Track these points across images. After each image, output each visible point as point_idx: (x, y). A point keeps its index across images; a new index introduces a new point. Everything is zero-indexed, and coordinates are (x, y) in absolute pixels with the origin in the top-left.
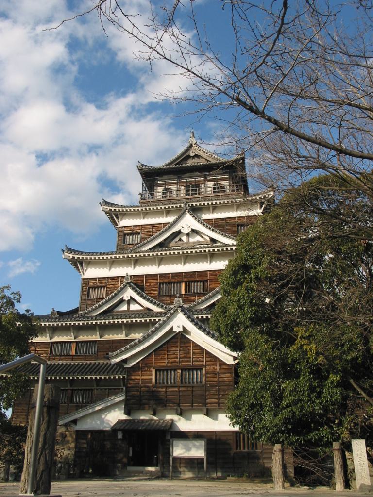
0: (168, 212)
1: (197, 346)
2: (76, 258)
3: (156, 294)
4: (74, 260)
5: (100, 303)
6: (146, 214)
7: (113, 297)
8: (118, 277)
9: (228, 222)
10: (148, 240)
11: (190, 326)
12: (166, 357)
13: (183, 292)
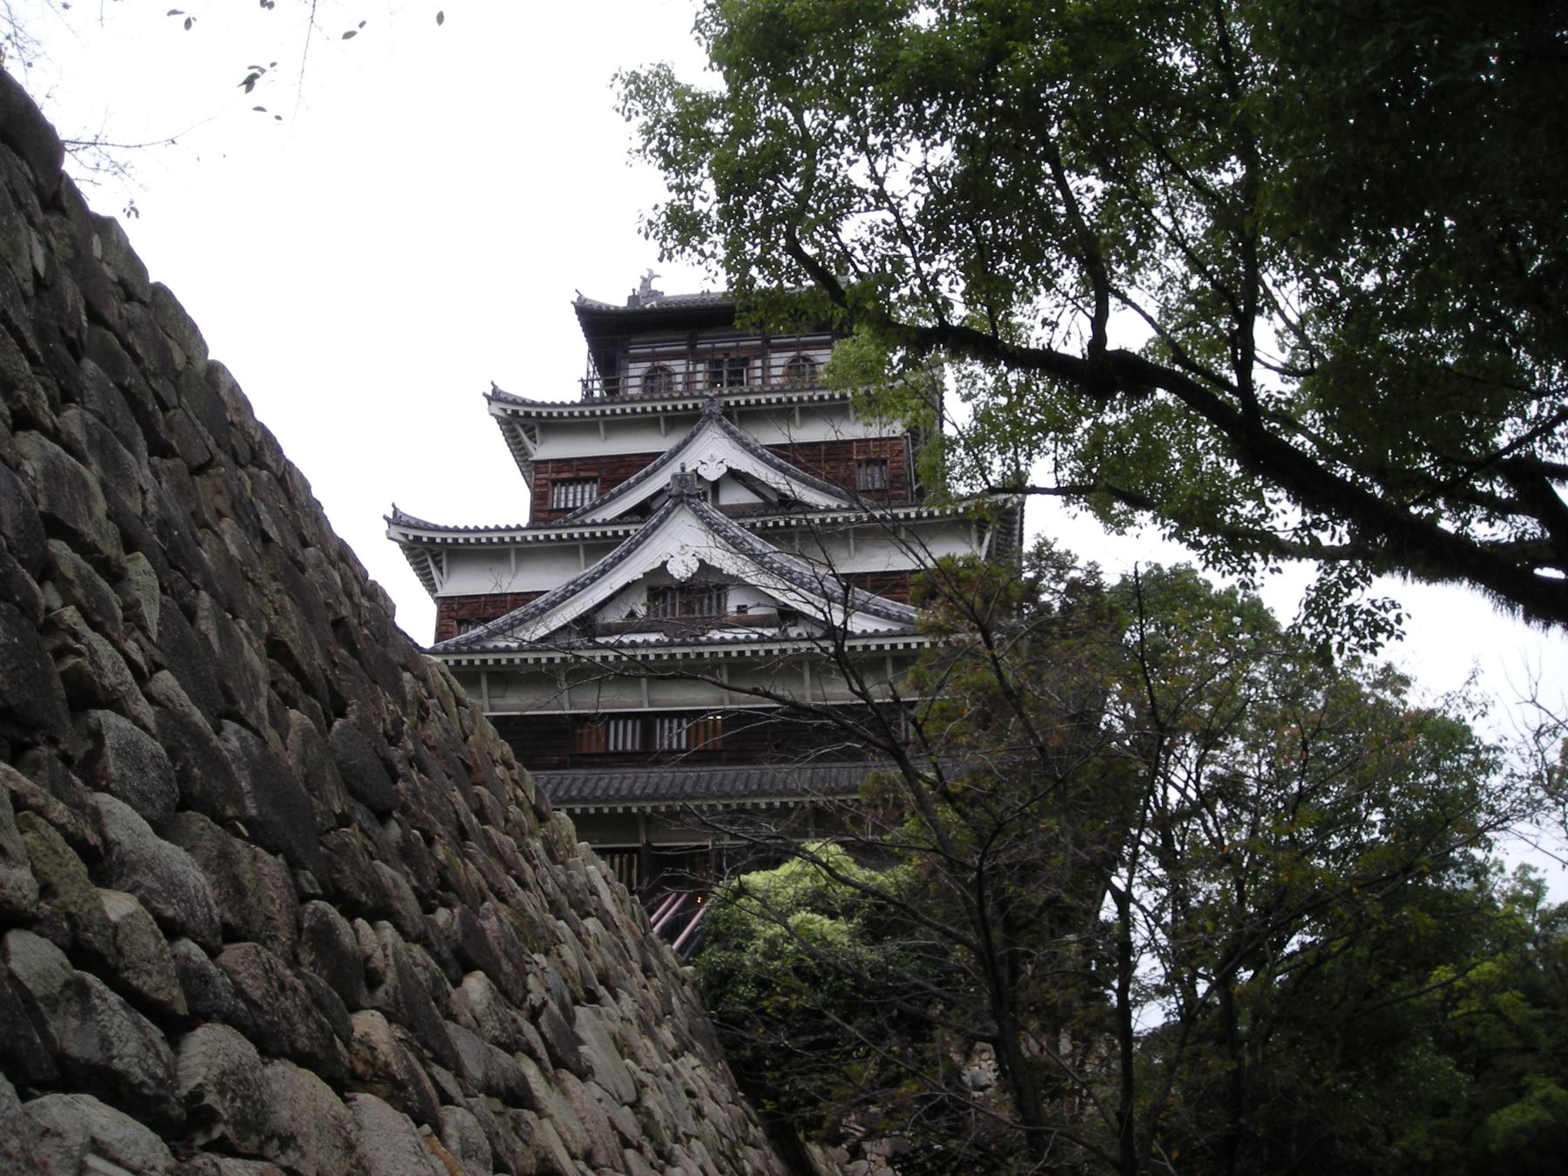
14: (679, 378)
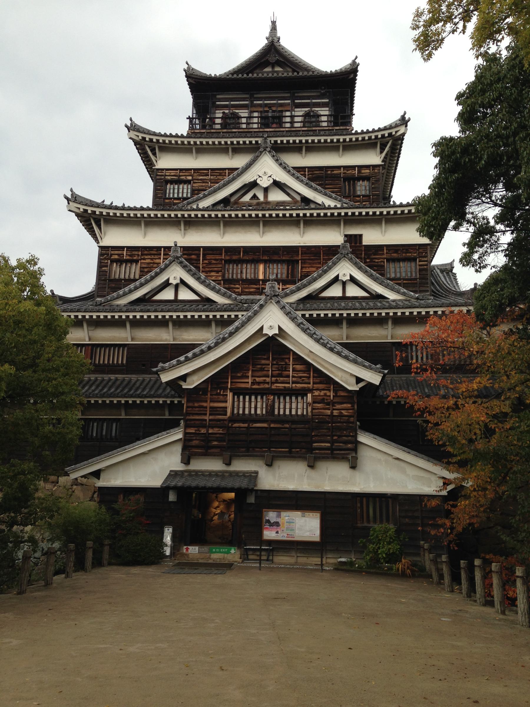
0: (237, 150)
1: (299, 359)
2: (89, 212)
3: (220, 278)
4: (85, 215)
5: (132, 286)
6: (201, 150)
7: (152, 278)
8: (158, 248)
9: (329, 172)
10: (206, 193)
11: (290, 327)
12: (250, 373)
13: (261, 277)
14: (244, 120)
